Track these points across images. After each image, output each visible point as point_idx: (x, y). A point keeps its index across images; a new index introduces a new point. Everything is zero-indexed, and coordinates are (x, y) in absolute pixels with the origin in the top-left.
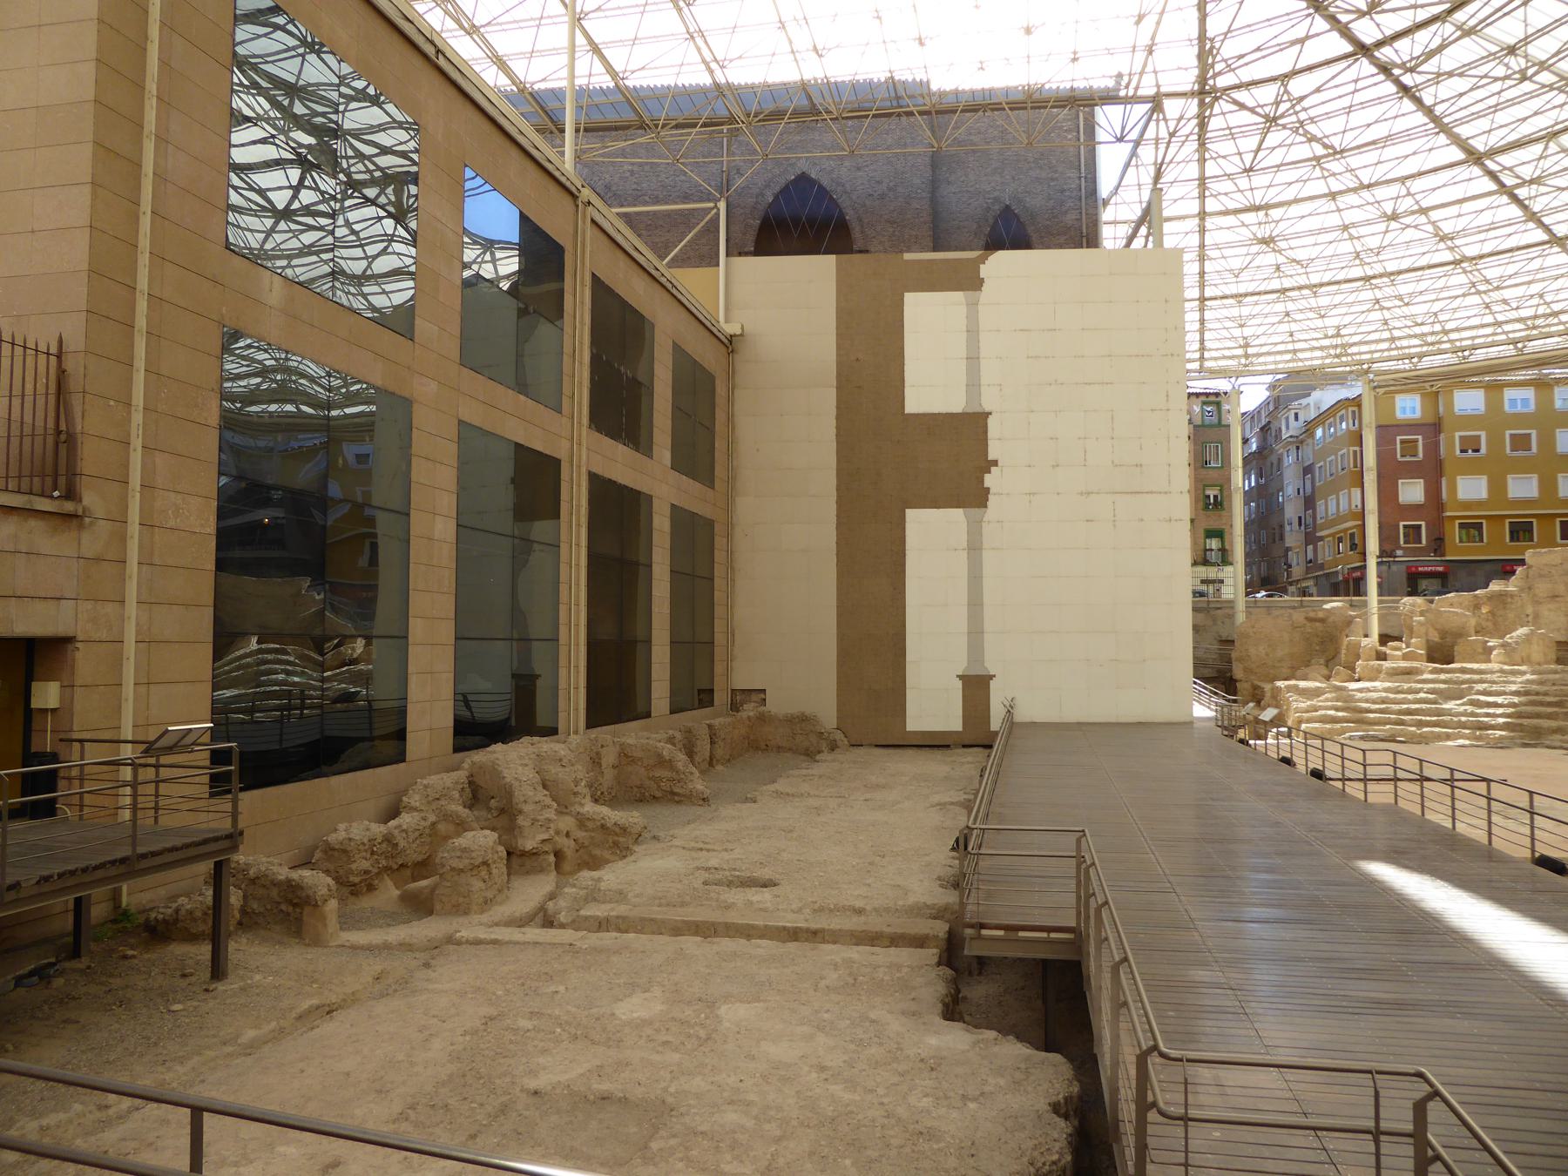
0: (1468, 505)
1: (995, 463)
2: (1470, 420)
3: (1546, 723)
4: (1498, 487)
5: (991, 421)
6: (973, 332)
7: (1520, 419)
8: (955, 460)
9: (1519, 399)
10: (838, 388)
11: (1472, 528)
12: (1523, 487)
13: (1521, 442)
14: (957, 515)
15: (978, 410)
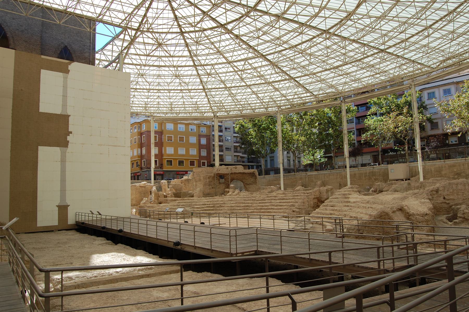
0: (169, 155)
1: (71, 133)
2: (170, 132)
3: (212, 212)
4: (176, 151)
5: (70, 118)
6: (65, 87)
7: (181, 133)
8: (57, 130)
9: (182, 128)
10: (14, 99)
11: (170, 162)
12: (182, 151)
13: (181, 139)
14: (57, 149)
15: (65, 114)
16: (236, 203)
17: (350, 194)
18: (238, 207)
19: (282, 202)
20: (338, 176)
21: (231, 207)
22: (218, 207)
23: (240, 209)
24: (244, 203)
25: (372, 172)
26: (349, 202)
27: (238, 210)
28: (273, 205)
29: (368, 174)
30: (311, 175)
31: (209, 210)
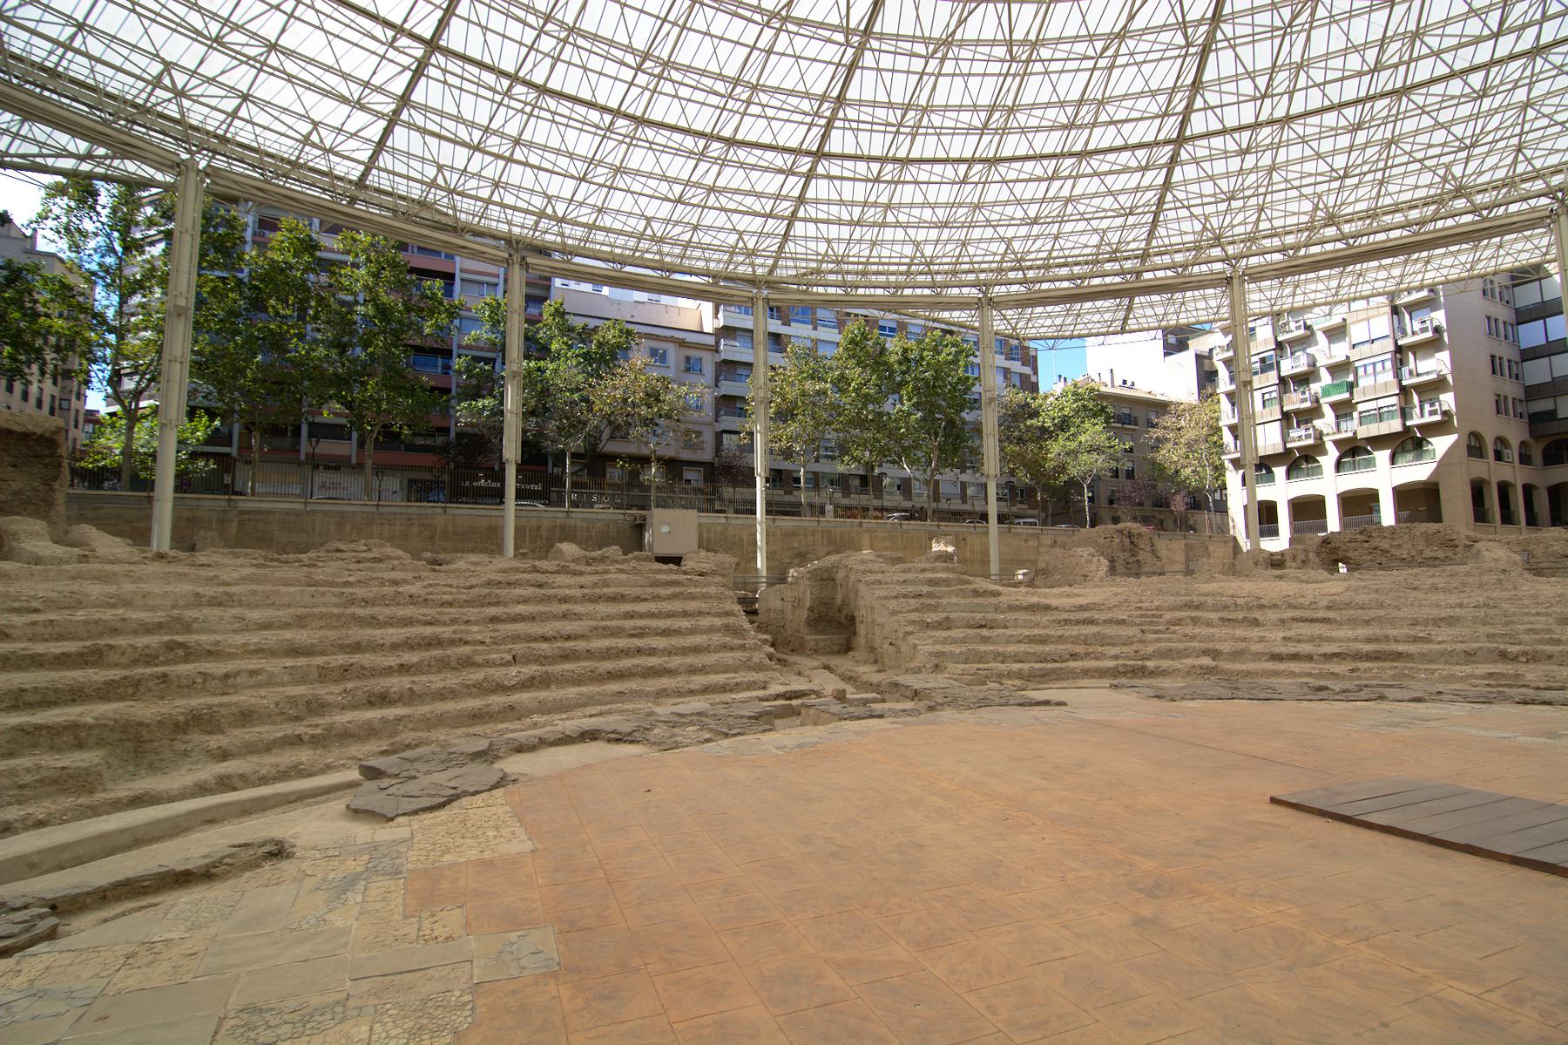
16: (300, 622)
17: (969, 582)
18: (357, 648)
19: (642, 616)
20: (415, 530)
21: (294, 651)
22: (149, 658)
23: (404, 669)
24: (373, 622)
25: (562, 527)
26: (1048, 608)
27: (388, 671)
28: (616, 633)
29: (544, 533)
30: (259, 512)
31: (76, 695)
